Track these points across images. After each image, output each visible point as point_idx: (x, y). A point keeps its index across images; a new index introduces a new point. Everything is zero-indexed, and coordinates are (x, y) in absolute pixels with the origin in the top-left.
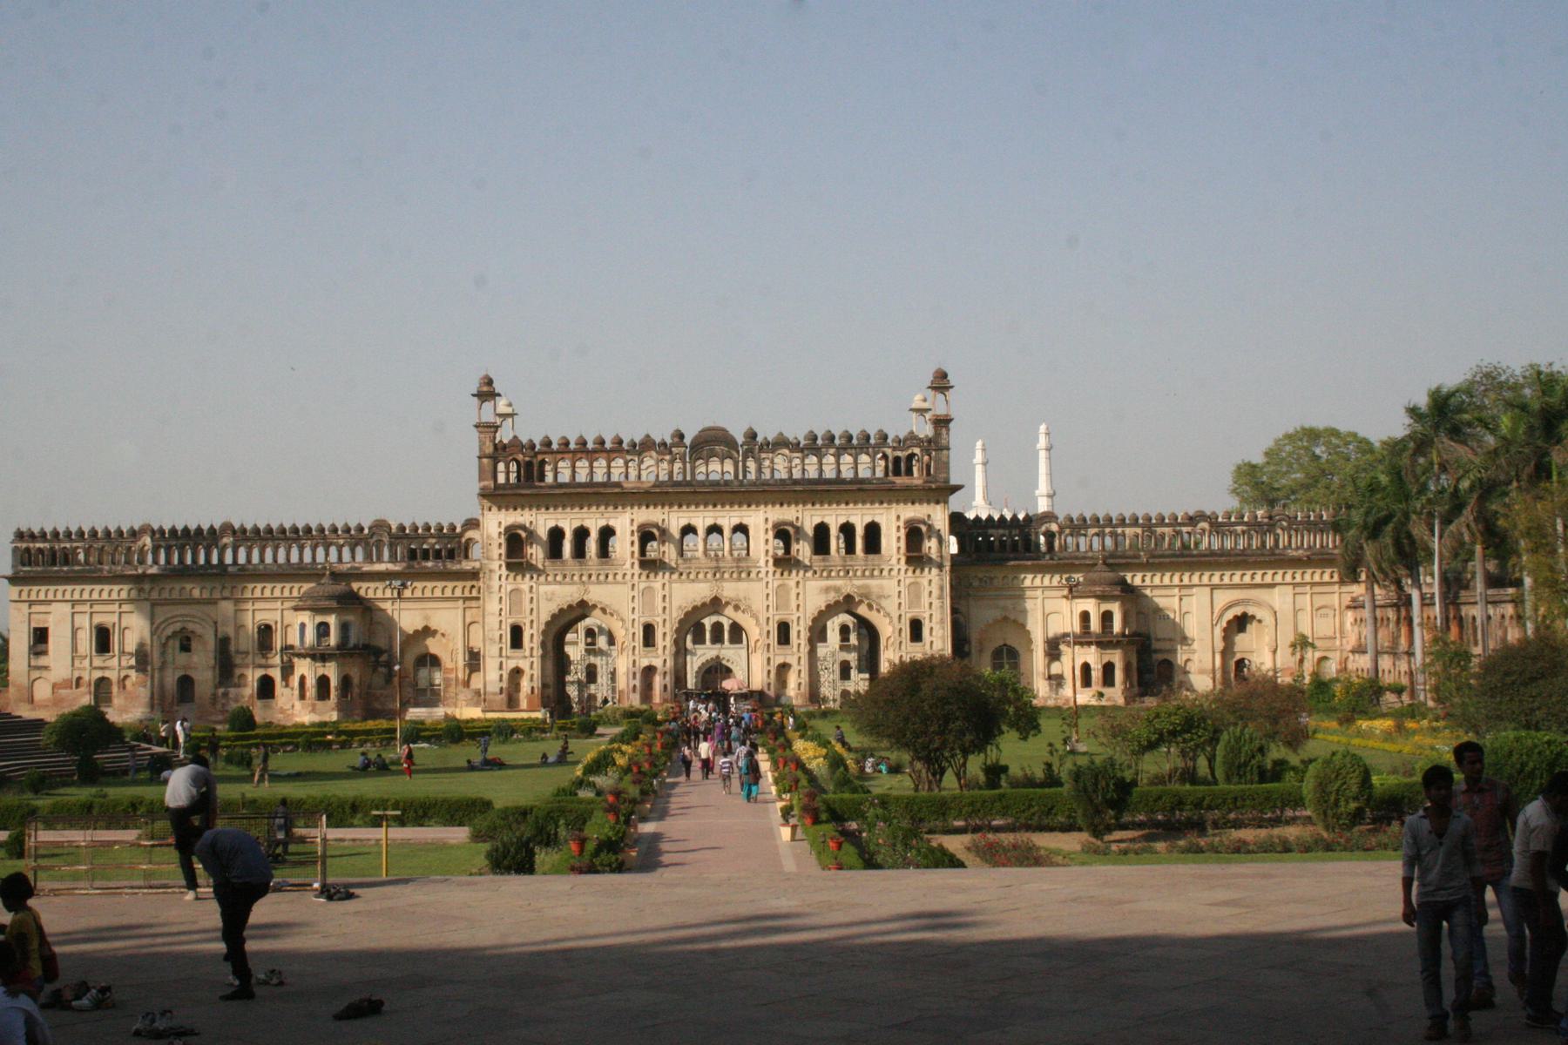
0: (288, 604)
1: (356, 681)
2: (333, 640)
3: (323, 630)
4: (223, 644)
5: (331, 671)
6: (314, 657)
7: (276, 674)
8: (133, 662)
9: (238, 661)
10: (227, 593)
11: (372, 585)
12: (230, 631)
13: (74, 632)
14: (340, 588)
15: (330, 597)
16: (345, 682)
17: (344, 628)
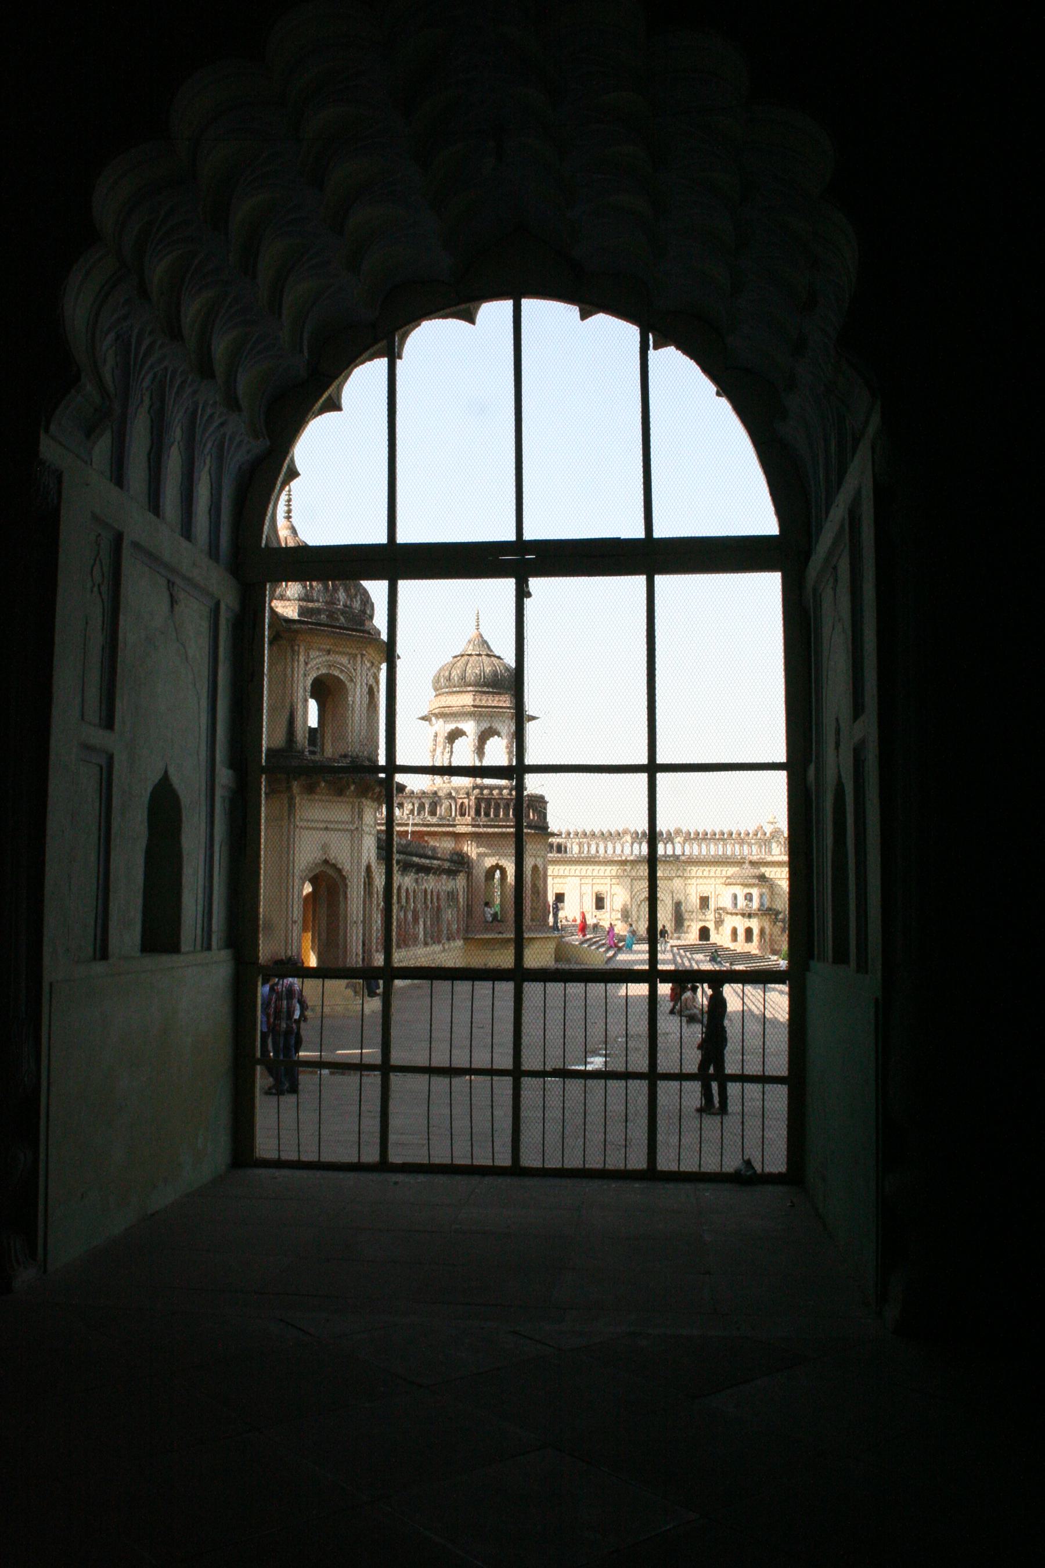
0: (719, 881)
1: (767, 931)
2: (755, 904)
3: (749, 897)
4: (678, 905)
5: (754, 924)
6: (743, 915)
7: (711, 926)
8: (619, 916)
9: (686, 916)
10: (680, 873)
11: (775, 869)
12: (682, 898)
13: (581, 896)
14: (756, 872)
15: (754, 877)
16: (762, 932)
17: (761, 896)
